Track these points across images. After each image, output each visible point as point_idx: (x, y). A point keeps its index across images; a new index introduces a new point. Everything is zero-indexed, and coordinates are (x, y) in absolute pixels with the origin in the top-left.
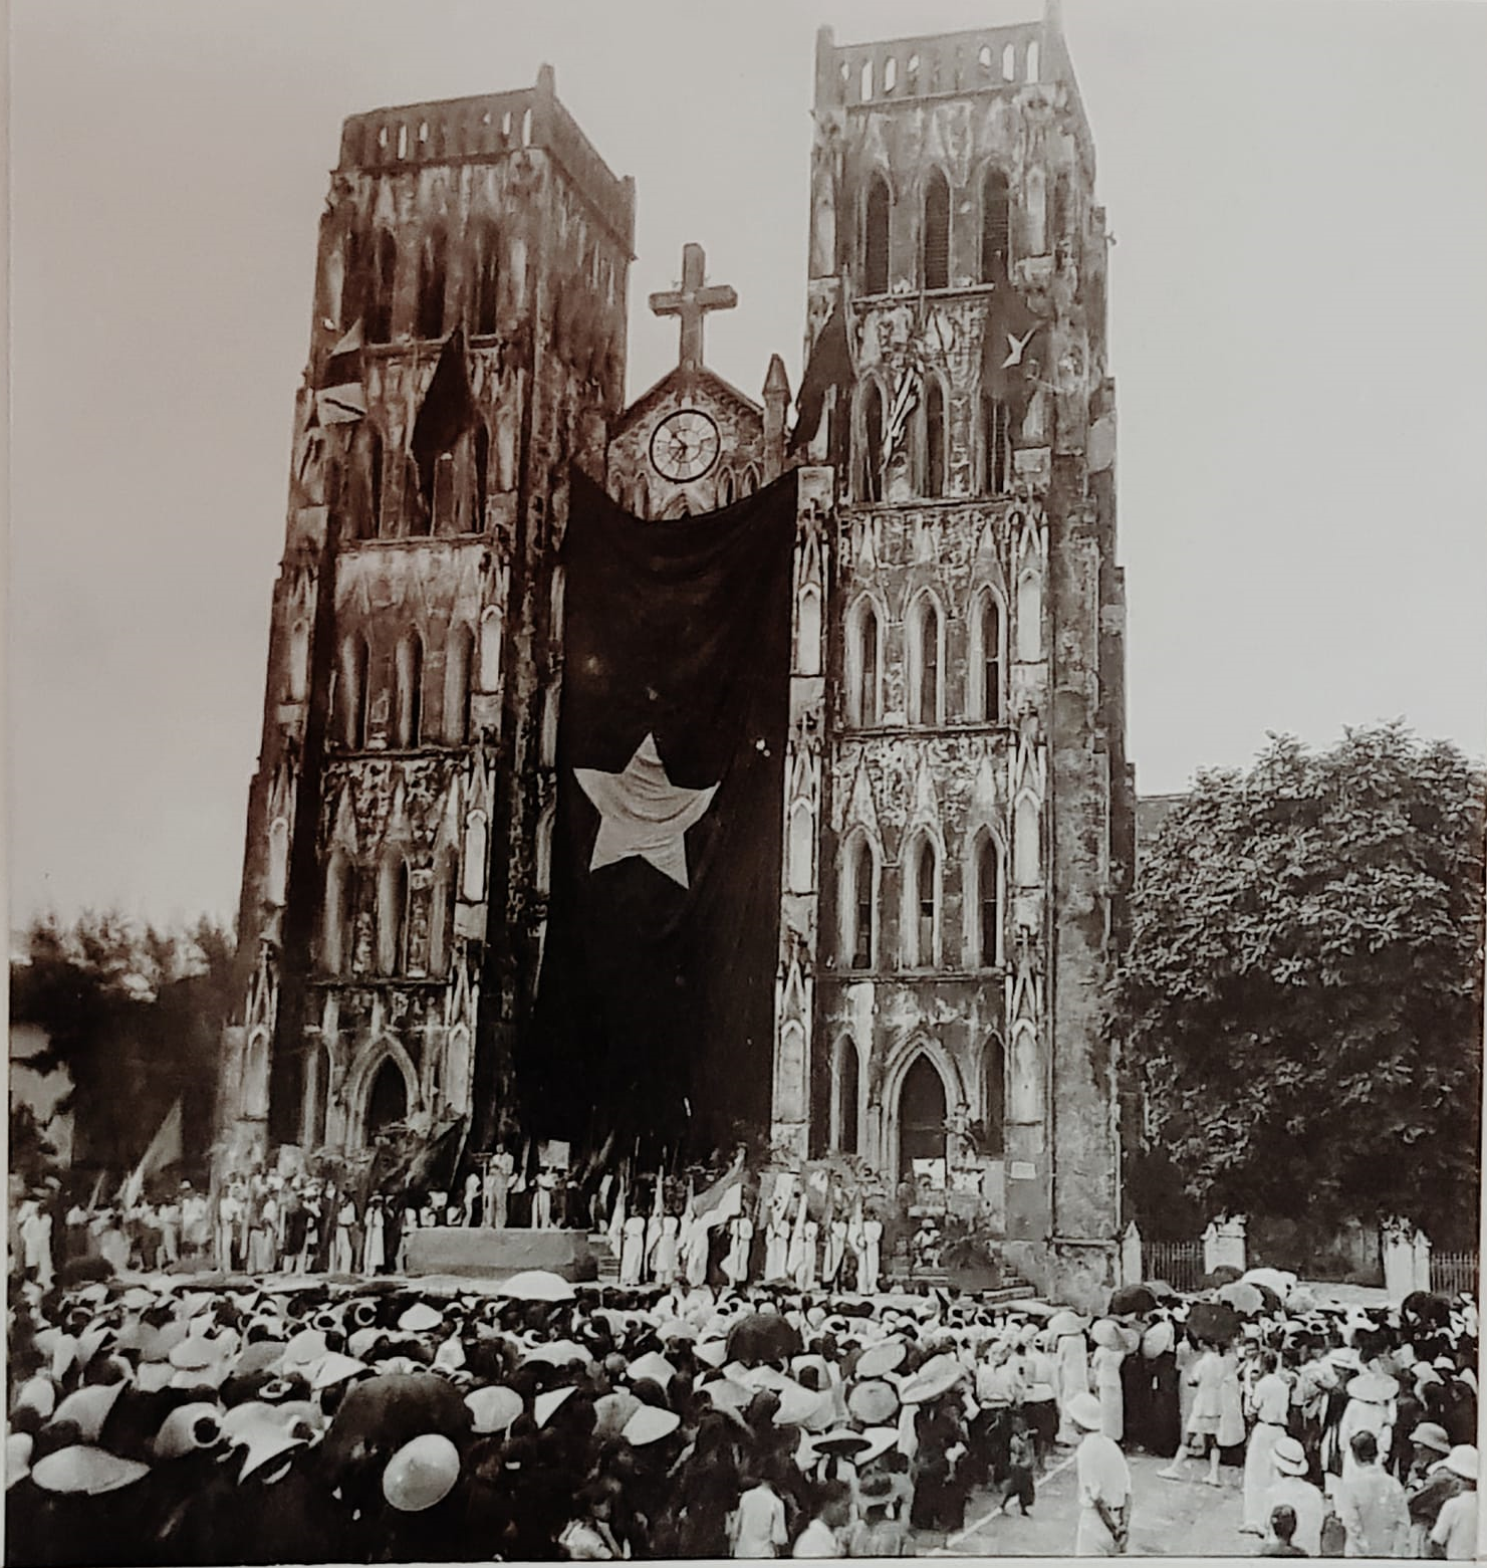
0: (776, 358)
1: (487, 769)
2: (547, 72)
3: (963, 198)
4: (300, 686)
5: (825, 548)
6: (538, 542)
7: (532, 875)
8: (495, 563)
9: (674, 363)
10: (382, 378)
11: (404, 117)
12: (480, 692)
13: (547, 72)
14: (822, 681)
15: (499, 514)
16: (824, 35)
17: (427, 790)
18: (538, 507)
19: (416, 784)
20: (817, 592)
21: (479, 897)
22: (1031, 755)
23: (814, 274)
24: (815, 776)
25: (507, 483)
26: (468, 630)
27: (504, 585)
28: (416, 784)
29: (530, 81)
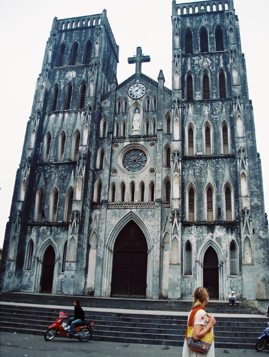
0: (161, 71)
1: (83, 165)
2: (105, 11)
3: (210, 33)
4: (32, 146)
5: (180, 109)
6: (98, 112)
7: (92, 196)
8: (87, 114)
9: (134, 73)
10: (60, 75)
11: (70, 20)
12: (82, 145)
13: (105, 11)
14: (180, 142)
15: (89, 103)
16: (174, 2)
17: (65, 172)
18: (98, 104)
19: (62, 171)
20: (178, 119)
21: (80, 199)
22: (244, 161)
23: (174, 48)
24: (180, 167)
25: (92, 95)
26: (79, 132)
27: (90, 117)
28: (62, 171)
29: (101, 12)
